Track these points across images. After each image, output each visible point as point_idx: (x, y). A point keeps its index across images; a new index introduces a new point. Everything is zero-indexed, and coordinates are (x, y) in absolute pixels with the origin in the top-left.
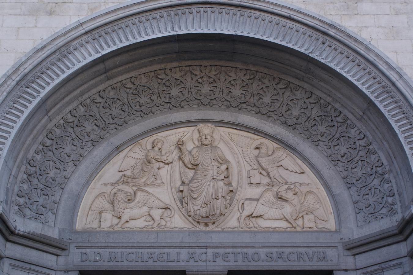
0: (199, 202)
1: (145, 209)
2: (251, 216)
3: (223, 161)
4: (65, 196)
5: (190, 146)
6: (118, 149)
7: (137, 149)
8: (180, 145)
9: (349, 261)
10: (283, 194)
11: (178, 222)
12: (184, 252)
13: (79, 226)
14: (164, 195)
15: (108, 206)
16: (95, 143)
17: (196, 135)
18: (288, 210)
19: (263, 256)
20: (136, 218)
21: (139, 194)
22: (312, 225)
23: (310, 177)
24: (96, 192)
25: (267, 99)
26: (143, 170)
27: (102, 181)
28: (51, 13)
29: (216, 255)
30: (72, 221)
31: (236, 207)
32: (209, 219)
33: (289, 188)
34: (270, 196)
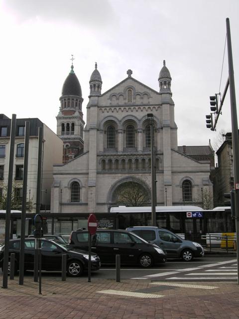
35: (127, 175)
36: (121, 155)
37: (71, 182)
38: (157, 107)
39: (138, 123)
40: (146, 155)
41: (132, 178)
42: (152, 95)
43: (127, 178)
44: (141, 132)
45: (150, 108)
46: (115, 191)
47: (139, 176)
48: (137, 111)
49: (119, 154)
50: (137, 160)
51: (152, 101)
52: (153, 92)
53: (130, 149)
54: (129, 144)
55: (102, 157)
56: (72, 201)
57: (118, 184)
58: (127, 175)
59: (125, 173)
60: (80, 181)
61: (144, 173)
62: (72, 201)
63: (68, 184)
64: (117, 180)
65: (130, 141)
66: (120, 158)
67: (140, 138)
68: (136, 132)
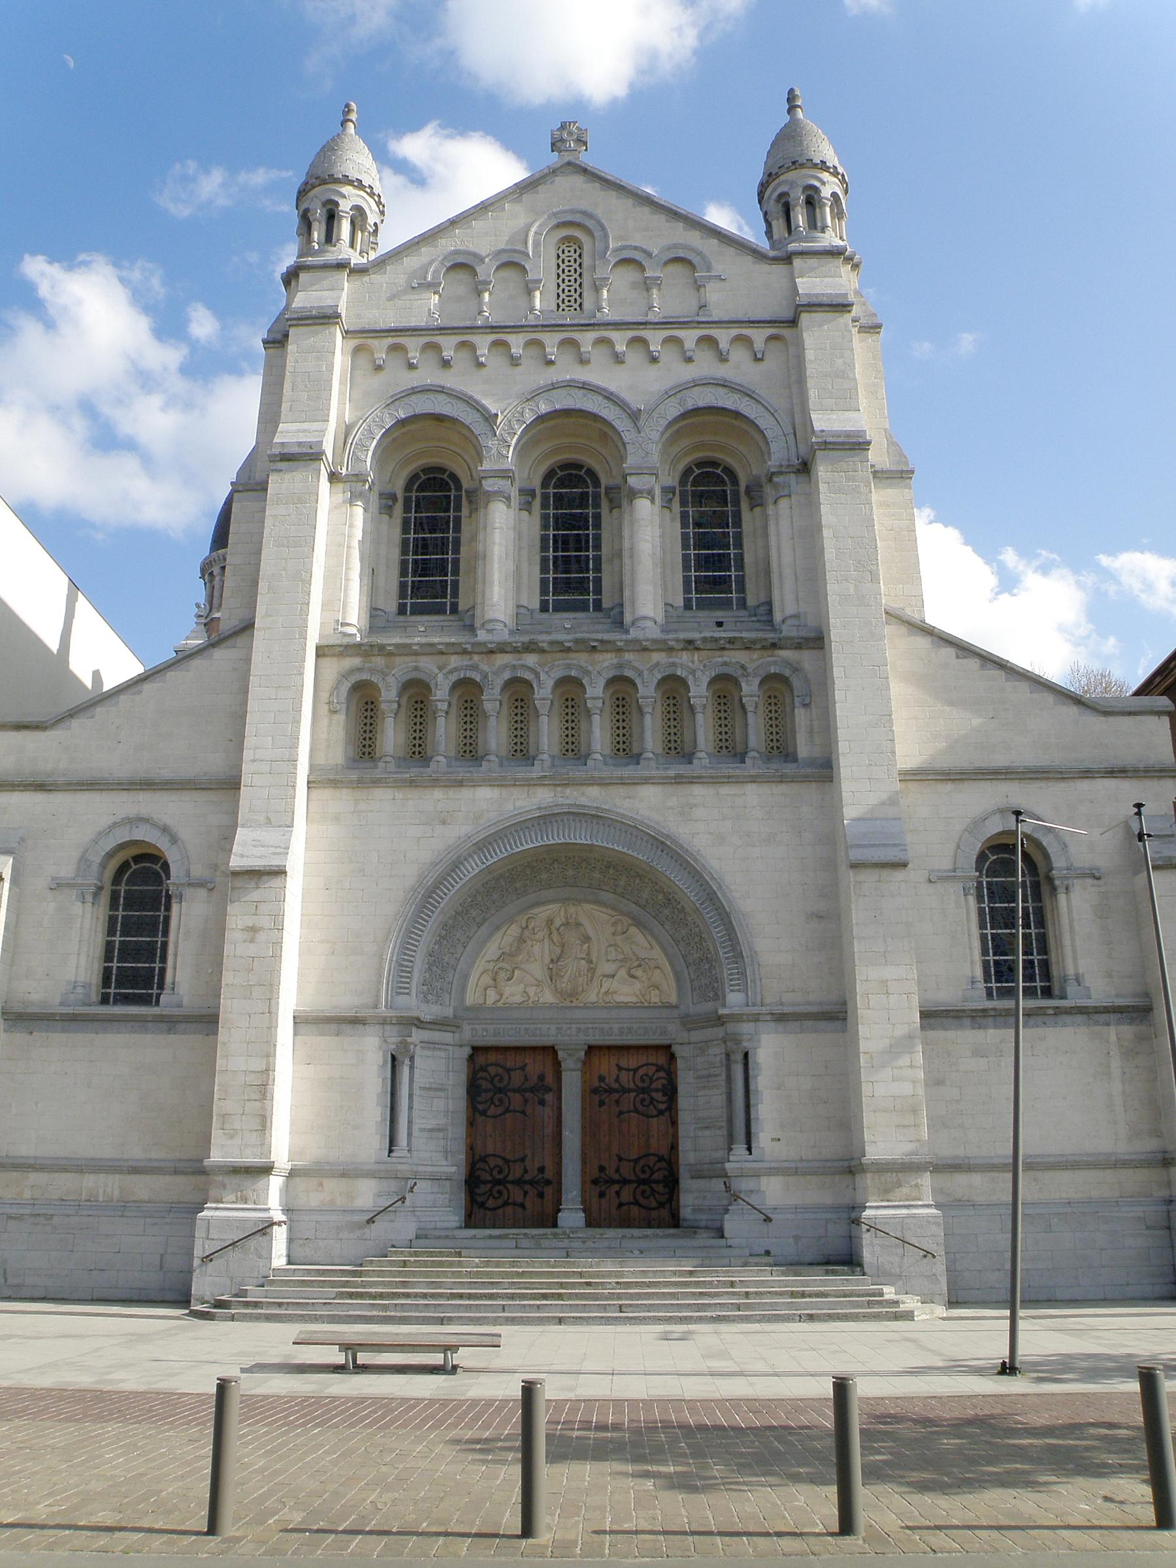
0: (565, 980)
1: (522, 986)
2: (607, 993)
3: (587, 939)
4: (457, 976)
5: (557, 923)
6: (498, 928)
7: (514, 927)
8: (550, 921)
9: (684, 1036)
10: (633, 971)
12: (553, 1027)
13: (471, 998)
14: (537, 970)
15: (491, 982)
16: (479, 925)
17: (562, 913)
18: (638, 986)
19: (616, 1031)
20: (513, 993)
21: (517, 972)
22: (657, 1000)
23: (657, 954)
24: (481, 969)
25: (622, 883)
27: (488, 958)
28: (444, 823)
29: (579, 1030)
32: (573, 994)
33: (640, 966)
34: (623, 973)
35: (543, 797)
36: (502, 648)
37: (109, 844)
38: (759, 336)
39: (627, 437)
40: (690, 645)
41: (579, 815)
42: (725, 262)
43: (546, 819)
44: (650, 494)
46: (446, 934)
47: (649, 803)
48: (618, 359)
49: (482, 636)
50: (621, 687)
51: (722, 300)
52: (731, 251)
53: (567, 619)
54: (563, 586)
55: (356, 661)
56: (105, 1000)
57: (473, 868)
58: (543, 797)
59: (530, 784)
60: (174, 840)
61: (679, 780)
62: (105, 1000)
63: (83, 860)
64: (460, 830)
65: (563, 564)
66: (495, 672)
67: (648, 544)
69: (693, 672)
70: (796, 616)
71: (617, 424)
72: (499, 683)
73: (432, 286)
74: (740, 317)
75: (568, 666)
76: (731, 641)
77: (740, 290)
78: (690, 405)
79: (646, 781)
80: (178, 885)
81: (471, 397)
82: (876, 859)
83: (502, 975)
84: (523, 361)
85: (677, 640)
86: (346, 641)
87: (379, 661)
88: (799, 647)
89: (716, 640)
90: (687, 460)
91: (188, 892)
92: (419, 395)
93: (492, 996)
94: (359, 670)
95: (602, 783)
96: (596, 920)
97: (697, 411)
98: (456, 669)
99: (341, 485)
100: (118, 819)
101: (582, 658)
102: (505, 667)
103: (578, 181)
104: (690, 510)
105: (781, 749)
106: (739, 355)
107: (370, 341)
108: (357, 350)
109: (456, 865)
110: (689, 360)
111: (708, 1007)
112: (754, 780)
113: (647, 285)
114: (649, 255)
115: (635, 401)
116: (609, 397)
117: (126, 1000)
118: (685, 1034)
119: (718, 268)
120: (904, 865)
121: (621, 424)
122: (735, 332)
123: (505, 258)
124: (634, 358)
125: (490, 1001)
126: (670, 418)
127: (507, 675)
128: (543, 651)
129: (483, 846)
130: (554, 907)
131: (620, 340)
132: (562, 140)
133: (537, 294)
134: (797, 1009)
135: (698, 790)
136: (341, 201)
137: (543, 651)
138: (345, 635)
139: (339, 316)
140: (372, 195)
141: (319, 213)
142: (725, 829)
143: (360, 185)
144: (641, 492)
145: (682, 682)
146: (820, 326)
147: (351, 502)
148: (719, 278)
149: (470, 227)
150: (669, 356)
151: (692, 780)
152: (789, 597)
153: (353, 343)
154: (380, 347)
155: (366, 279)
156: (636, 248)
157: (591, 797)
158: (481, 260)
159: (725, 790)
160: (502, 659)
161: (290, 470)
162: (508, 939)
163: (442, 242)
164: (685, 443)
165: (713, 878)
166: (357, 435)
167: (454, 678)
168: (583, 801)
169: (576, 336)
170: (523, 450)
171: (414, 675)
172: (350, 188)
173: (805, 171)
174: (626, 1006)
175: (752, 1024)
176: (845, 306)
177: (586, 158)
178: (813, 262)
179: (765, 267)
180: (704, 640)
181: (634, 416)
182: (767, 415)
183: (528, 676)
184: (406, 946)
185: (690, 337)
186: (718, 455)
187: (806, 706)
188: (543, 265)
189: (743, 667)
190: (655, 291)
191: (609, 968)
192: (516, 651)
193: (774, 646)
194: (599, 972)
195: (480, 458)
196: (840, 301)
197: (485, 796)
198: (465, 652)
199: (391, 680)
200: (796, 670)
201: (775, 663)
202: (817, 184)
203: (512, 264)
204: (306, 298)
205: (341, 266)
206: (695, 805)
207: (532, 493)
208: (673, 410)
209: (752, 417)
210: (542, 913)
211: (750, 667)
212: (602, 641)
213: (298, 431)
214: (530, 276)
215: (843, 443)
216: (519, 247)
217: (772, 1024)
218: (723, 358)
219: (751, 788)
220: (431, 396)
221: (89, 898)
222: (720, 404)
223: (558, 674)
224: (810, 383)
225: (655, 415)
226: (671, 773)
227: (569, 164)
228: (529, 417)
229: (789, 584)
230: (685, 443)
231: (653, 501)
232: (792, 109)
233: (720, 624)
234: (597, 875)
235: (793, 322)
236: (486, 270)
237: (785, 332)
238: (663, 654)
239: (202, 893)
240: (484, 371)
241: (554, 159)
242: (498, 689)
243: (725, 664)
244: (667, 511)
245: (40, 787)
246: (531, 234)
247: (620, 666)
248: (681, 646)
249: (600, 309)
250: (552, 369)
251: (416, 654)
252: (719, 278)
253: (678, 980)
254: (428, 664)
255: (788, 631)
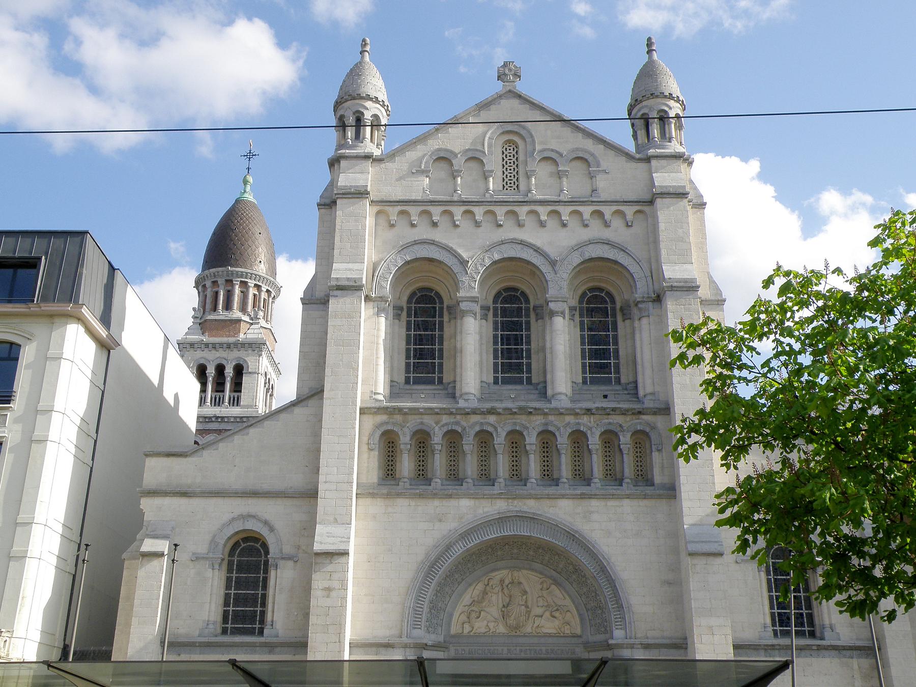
0: (512, 618)
3: (525, 592)
5: (507, 582)
6: (470, 585)
10: (554, 614)
11: (501, 629)
14: (494, 611)
15: (466, 619)
16: (459, 584)
18: (557, 623)
19: (544, 651)
20: (480, 626)
22: (569, 632)
23: (568, 602)
25: (547, 558)
26: (483, 598)
28: (440, 521)
29: (521, 651)
30: (449, 631)
31: (531, 620)
32: (517, 627)
33: (557, 610)
34: (547, 614)
35: (501, 506)
36: (474, 412)
37: (230, 531)
38: (629, 211)
39: (549, 277)
40: (589, 411)
41: (522, 517)
42: (608, 161)
43: (502, 520)
44: (563, 313)
45: (599, 214)
46: (440, 591)
47: (564, 510)
48: (542, 224)
49: (462, 404)
50: (547, 439)
51: (607, 187)
52: (611, 153)
53: (511, 390)
54: (507, 368)
55: (384, 418)
56: (224, 631)
57: (459, 550)
58: (501, 506)
59: (492, 497)
60: (272, 529)
61: (583, 496)
62: (224, 631)
63: (213, 542)
64: (451, 526)
65: (507, 354)
66: (471, 426)
67: (561, 343)
68: (539, 317)
69: (590, 429)
70: (653, 394)
71: (542, 268)
72: (473, 433)
73: (425, 172)
74: (618, 198)
75: (515, 424)
76: (614, 409)
77: (618, 180)
78: (587, 256)
79: (563, 496)
80: (275, 559)
81: (451, 248)
82: (704, 551)
83: (474, 615)
84: (483, 224)
85: (581, 409)
86: (377, 405)
87: (399, 418)
88: (655, 413)
89: (605, 409)
90: (584, 288)
91: (281, 563)
92: (419, 246)
93: (467, 628)
94: (387, 423)
95: (537, 498)
96: (530, 579)
97: (591, 260)
98: (446, 424)
99: (371, 304)
100: (235, 515)
101: (523, 419)
102: (476, 423)
103: (515, 102)
104: (586, 320)
105: (644, 478)
106: (617, 223)
107: (387, 208)
108: (378, 213)
109: (448, 547)
110: (586, 226)
111: (600, 637)
112: (628, 497)
113: (559, 175)
114: (561, 155)
115: (553, 253)
116: (537, 250)
117: (236, 632)
118: (586, 654)
119: (604, 165)
120: (721, 555)
121: (545, 268)
122: (614, 208)
123: (470, 155)
124: (552, 223)
125: (466, 631)
126: (575, 265)
127: (477, 428)
128: (499, 414)
129: (465, 535)
130: (505, 572)
131: (543, 211)
132: (505, 74)
133: (491, 179)
134: (657, 641)
135: (594, 503)
136: (365, 112)
137: (499, 414)
138: (377, 400)
139: (368, 193)
140: (383, 106)
141: (351, 120)
142: (610, 527)
143: (376, 100)
144: (557, 312)
145: (584, 434)
146: (668, 207)
147: (378, 315)
148: (605, 172)
149: (448, 132)
150: (573, 223)
151: (591, 497)
152: (648, 382)
153: (376, 209)
154: (393, 211)
155: (383, 165)
156: (552, 150)
157: (530, 506)
158: (456, 155)
159: (611, 503)
160: (475, 418)
161: (343, 297)
162: (476, 592)
163: (430, 142)
164: (583, 277)
165: (604, 558)
166: (380, 271)
167: (445, 429)
168: (525, 509)
169: (516, 209)
170: (483, 282)
171: (420, 427)
172: (370, 103)
173: (659, 100)
174: (550, 635)
175: (630, 650)
176: (684, 194)
177: (521, 87)
178: (663, 162)
179: (633, 165)
180: (597, 408)
181: (553, 263)
182: (635, 263)
183: (490, 429)
184: (418, 599)
185: (587, 210)
186: (603, 285)
187: (659, 450)
188: (494, 161)
189: (621, 426)
190: (565, 179)
191: (539, 611)
192: (483, 413)
193: (640, 413)
194: (533, 614)
195: (457, 289)
196: (681, 191)
197: (465, 503)
198: (451, 413)
199: (406, 429)
200: (653, 428)
201: (640, 423)
202: (666, 109)
203: (475, 158)
204: (347, 178)
205: (367, 157)
206: (592, 512)
207: (488, 309)
208: (576, 259)
209: (626, 265)
210: (498, 575)
211: (625, 426)
212: (535, 409)
213: (346, 269)
214: (486, 168)
215: (683, 287)
216: (479, 148)
217: (642, 650)
218: (607, 225)
219: (626, 502)
220: (426, 246)
221: (217, 566)
222: (606, 256)
223: (509, 428)
224: (662, 245)
225: (566, 262)
226: (579, 492)
227: (510, 91)
228: (488, 262)
229: (648, 372)
230: (583, 277)
231: (564, 318)
232: (650, 52)
233: (605, 397)
234: (531, 553)
235: (651, 202)
236: (458, 163)
237: (646, 208)
238: (572, 417)
239: (290, 563)
240: (458, 230)
241: (499, 87)
242: (471, 438)
243: (610, 423)
244: (572, 322)
245: (184, 494)
246: (487, 139)
247: (546, 424)
248: (583, 412)
249: (530, 191)
250: (501, 229)
251: (422, 414)
252: (605, 172)
253: (582, 620)
254: (429, 420)
255: (648, 404)
